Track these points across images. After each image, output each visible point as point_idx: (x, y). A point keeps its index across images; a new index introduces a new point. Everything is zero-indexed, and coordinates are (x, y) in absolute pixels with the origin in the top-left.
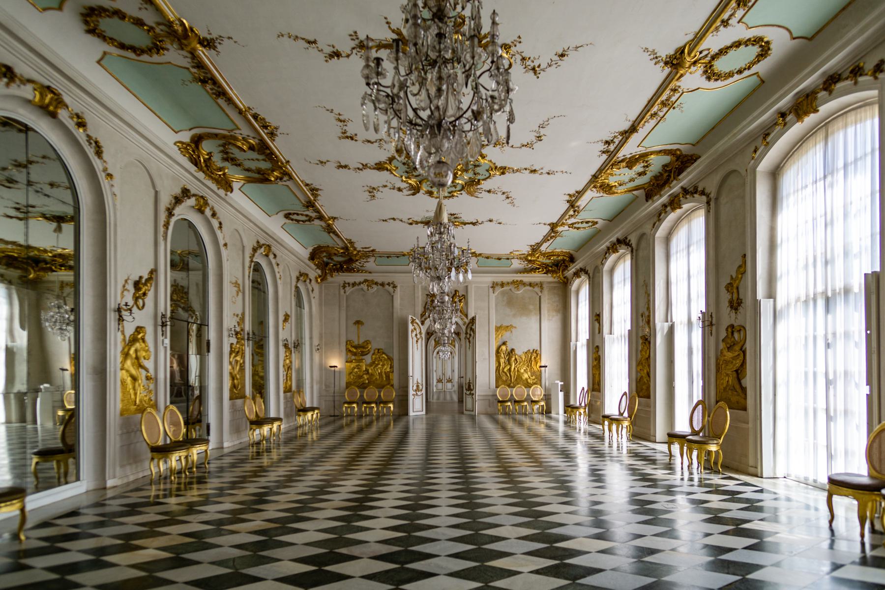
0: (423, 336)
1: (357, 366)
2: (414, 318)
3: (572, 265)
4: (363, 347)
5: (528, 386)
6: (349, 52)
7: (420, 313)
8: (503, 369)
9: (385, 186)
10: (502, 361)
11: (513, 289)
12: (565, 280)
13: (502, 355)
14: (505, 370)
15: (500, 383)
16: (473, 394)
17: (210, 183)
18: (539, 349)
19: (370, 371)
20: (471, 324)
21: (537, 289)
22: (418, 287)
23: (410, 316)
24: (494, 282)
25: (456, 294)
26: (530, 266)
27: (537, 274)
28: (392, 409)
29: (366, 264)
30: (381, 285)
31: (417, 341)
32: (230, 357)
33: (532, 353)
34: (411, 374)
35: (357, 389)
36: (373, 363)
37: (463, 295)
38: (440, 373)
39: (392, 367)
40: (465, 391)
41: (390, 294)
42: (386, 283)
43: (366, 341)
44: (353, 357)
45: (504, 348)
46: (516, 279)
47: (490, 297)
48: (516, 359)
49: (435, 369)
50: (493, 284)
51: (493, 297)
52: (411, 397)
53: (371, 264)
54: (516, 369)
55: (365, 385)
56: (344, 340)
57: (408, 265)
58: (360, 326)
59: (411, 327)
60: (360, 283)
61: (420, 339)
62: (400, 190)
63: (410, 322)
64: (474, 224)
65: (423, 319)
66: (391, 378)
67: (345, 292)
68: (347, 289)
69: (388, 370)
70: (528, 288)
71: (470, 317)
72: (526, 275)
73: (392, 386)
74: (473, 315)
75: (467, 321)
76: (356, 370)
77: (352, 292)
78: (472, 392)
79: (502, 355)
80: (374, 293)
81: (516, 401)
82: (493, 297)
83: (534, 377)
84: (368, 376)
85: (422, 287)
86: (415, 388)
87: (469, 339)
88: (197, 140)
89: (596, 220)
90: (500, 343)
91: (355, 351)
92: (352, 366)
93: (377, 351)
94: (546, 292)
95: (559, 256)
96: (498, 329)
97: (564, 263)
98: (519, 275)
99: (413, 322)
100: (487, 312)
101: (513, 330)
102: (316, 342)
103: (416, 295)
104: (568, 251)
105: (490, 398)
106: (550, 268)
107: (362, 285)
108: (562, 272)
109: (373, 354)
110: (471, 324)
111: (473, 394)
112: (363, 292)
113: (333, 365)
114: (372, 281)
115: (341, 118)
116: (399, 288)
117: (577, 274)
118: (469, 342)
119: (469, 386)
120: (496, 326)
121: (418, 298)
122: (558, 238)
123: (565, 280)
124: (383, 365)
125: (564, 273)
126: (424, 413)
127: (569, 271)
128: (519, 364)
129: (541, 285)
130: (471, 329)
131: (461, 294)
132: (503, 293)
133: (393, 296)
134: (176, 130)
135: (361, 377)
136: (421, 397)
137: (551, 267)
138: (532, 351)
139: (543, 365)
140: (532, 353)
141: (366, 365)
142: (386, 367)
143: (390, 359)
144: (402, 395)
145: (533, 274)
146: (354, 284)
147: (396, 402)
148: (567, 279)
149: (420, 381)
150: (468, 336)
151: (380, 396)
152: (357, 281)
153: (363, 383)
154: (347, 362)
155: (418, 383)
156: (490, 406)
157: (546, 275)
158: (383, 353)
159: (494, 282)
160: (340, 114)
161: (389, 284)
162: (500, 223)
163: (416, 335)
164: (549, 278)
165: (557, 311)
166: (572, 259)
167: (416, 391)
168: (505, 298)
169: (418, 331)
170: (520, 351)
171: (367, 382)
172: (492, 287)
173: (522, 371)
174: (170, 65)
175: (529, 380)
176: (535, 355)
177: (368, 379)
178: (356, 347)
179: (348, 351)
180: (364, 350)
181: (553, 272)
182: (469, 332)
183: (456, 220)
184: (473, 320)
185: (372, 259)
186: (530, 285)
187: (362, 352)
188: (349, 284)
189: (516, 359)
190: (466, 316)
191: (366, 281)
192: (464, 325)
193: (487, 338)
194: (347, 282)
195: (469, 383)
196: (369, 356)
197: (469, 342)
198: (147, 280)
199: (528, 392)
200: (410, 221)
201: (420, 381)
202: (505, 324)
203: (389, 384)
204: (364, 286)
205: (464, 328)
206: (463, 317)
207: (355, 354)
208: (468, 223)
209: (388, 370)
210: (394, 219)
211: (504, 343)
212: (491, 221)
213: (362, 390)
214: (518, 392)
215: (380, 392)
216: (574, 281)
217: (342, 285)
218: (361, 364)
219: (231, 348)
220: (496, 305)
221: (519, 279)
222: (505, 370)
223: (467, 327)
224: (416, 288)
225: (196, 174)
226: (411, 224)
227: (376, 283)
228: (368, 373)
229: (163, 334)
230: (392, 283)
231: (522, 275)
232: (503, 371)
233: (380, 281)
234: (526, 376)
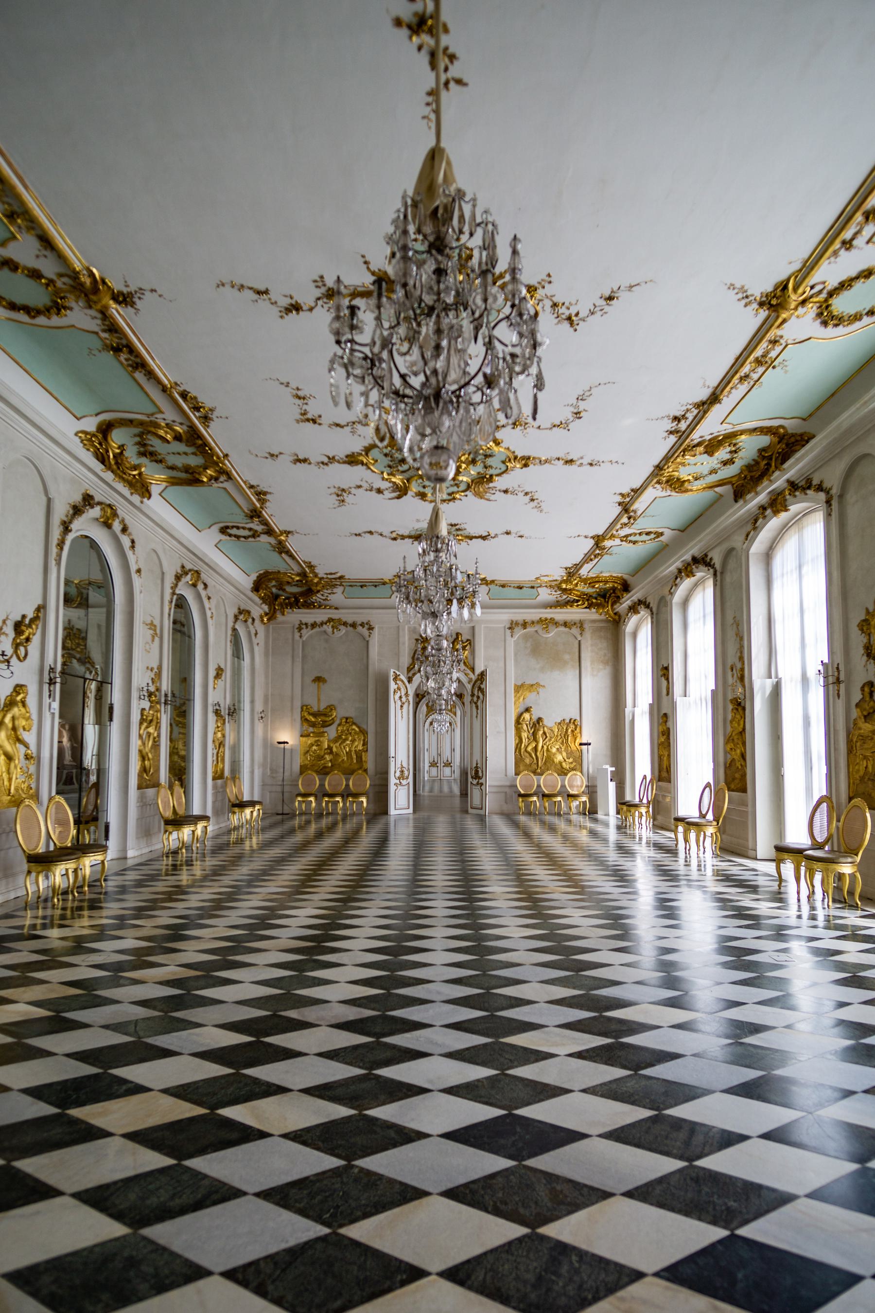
0: (411, 698)
1: (316, 741)
2: (398, 673)
3: (626, 596)
4: (325, 715)
5: (563, 772)
6: (313, 304)
7: (406, 665)
8: (526, 747)
9: (359, 487)
10: (524, 735)
11: (540, 631)
12: (617, 617)
13: (525, 727)
14: (529, 749)
15: (522, 768)
16: (482, 784)
17: (120, 487)
18: (578, 719)
19: (334, 749)
20: (479, 682)
21: (575, 631)
22: (404, 630)
23: (392, 671)
24: (512, 621)
25: (457, 638)
26: (565, 597)
27: (575, 609)
28: (365, 804)
29: (330, 597)
31: (402, 706)
32: (140, 728)
33: (568, 725)
34: (392, 754)
35: (315, 775)
36: (339, 737)
37: (468, 640)
38: (434, 753)
39: (365, 744)
40: (470, 780)
41: (364, 639)
42: (359, 623)
43: (329, 706)
44: (311, 729)
45: (527, 716)
46: (544, 616)
47: (507, 642)
48: (544, 733)
49: (426, 747)
50: (511, 624)
51: (511, 642)
52: (392, 788)
53: (337, 597)
54: (545, 747)
55: (327, 770)
56: (298, 704)
58: (321, 684)
59: (393, 686)
60: (322, 624)
61: (406, 704)
62: (379, 491)
63: (392, 678)
64: (484, 538)
65: (410, 675)
66: (364, 759)
67: (301, 637)
68: (304, 631)
69: (360, 747)
70: (562, 629)
71: (478, 671)
72: (558, 610)
73: (366, 771)
74: (482, 669)
75: (474, 678)
76: (314, 748)
77: (311, 636)
78: (481, 781)
79: (525, 727)
80: (341, 637)
81: (544, 795)
82: (511, 642)
83: (571, 760)
84: (331, 757)
85: (409, 628)
86: (398, 774)
87: (476, 703)
88: (105, 429)
89: (660, 530)
90: (522, 709)
91: (313, 720)
92: (309, 742)
93: (344, 720)
94: (588, 634)
95: (606, 582)
96: (518, 688)
97: (614, 592)
98: (549, 610)
99: (396, 678)
100: (502, 664)
101: (541, 690)
102: (259, 707)
103: (401, 640)
104: (620, 575)
105: (507, 790)
106: (594, 601)
107: (325, 626)
108: (612, 605)
109: (339, 725)
110: (479, 682)
111: (482, 784)
112: (326, 636)
113: (282, 740)
114: (339, 620)
115: (300, 393)
116: (376, 630)
117: (633, 609)
118: (477, 707)
119: (477, 772)
120: (515, 685)
121: (404, 644)
122: (605, 557)
123: (617, 617)
124: (353, 741)
125: (615, 607)
126: (411, 810)
127: (621, 604)
128: (550, 740)
129: (581, 625)
130: (480, 689)
131: (464, 638)
132: (526, 637)
134: (79, 416)
135: (321, 758)
136: (406, 787)
137: (596, 598)
138: (568, 721)
139: (584, 741)
140: (568, 725)
141: (329, 741)
142: (356, 743)
143: (363, 732)
144: (379, 785)
145: (569, 609)
146: (314, 625)
147: (371, 795)
148: (620, 616)
149: (405, 765)
150: (475, 699)
151: (347, 785)
152: (319, 620)
153: (325, 767)
154: (302, 736)
155: (402, 767)
156: (506, 802)
157: (587, 610)
158: (354, 724)
159: (512, 621)
160: (298, 389)
161: (362, 625)
162: (521, 536)
164: (592, 615)
165: (606, 663)
166: (626, 587)
167: (399, 778)
168: (529, 644)
169: (403, 692)
170: (550, 722)
171: (330, 765)
172: (510, 628)
173: (554, 750)
174: (72, 329)
175: (564, 764)
176: (572, 726)
177: (331, 761)
178: (314, 715)
179: (304, 720)
180: (327, 719)
181: (598, 606)
182: (476, 693)
183: (459, 533)
184: (482, 676)
185: (339, 590)
186: (565, 624)
187: (324, 722)
188: (306, 624)
189: (544, 733)
190: (473, 670)
191: (330, 620)
192: (470, 681)
193: (502, 702)
194: (304, 622)
195: (477, 767)
196: (334, 727)
197: (477, 707)
198: (32, 621)
199: (563, 781)
200: (394, 535)
201: (405, 765)
202: (528, 682)
203: (361, 768)
204: (328, 628)
205: (469, 687)
206: (468, 671)
207: (313, 725)
208: (476, 537)
209: (360, 747)
210: (371, 533)
211: (527, 710)
212: (508, 533)
213: (321, 776)
214: (548, 781)
215: (347, 780)
216: (629, 619)
218: (321, 739)
219: (142, 715)
220: (516, 655)
221: (549, 616)
222: (529, 749)
223: (474, 685)
225: (102, 474)
226: (395, 539)
227: (345, 624)
228: (331, 752)
229: (50, 696)
231: (553, 610)
232: (526, 751)
233: (350, 621)
234: (559, 758)
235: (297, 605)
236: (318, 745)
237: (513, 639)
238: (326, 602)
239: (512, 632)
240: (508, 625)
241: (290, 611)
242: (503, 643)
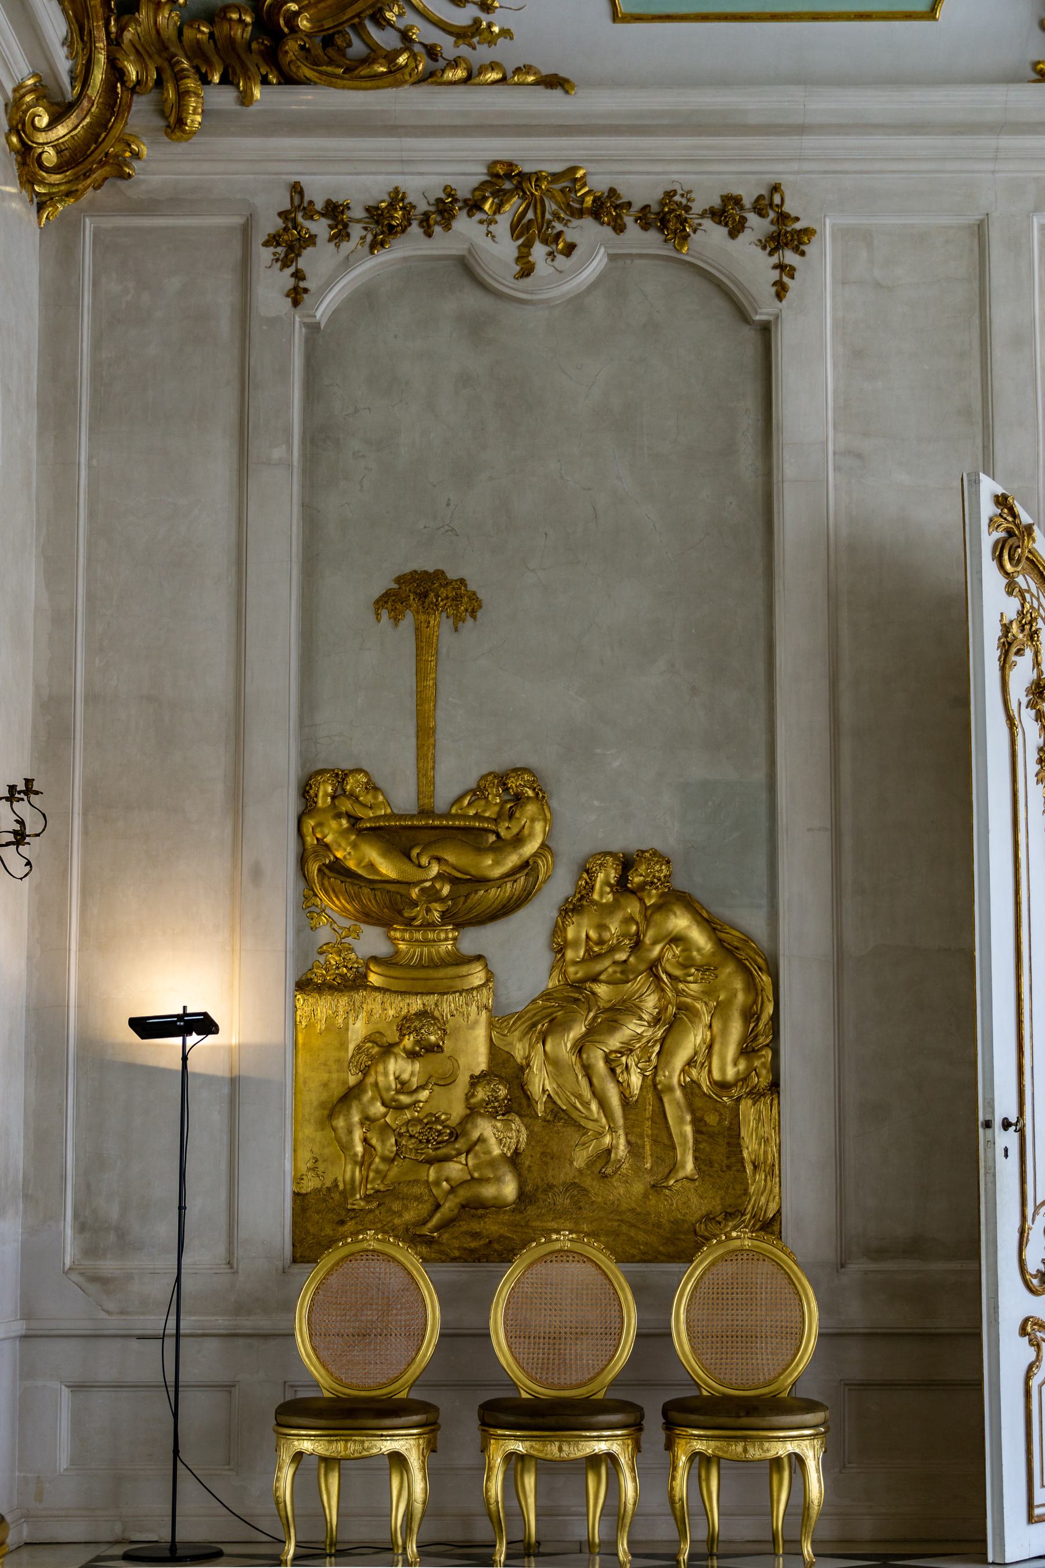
1: (405, 1024)
30: (646, 219)
35: (410, 1259)
42: (706, 198)
43: (501, 779)
55: (491, 1227)
58: (441, 625)
63: (988, 540)
66: (750, 1147)
67: (296, 295)
76: (397, 1067)
80: (577, 303)
84: (518, 1133)
91: (387, 869)
92: (358, 1029)
107: (464, 225)
112: (473, 300)
113: (168, 1006)
133: (766, 330)
141: (498, 1020)
153: (475, 1207)
154: (303, 985)
171: (509, 1189)
177: (514, 1160)
180: (492, 866)
188: (334, 211)
194: (317, 193)
203: (732, 1213)
213: (452, 1272)
217: (271, 224)
218: (448, 1005)
230: (760, 207)
235: (272, 57)
236: (425, 1051)
238: (483, 53)
241: (224, 98)
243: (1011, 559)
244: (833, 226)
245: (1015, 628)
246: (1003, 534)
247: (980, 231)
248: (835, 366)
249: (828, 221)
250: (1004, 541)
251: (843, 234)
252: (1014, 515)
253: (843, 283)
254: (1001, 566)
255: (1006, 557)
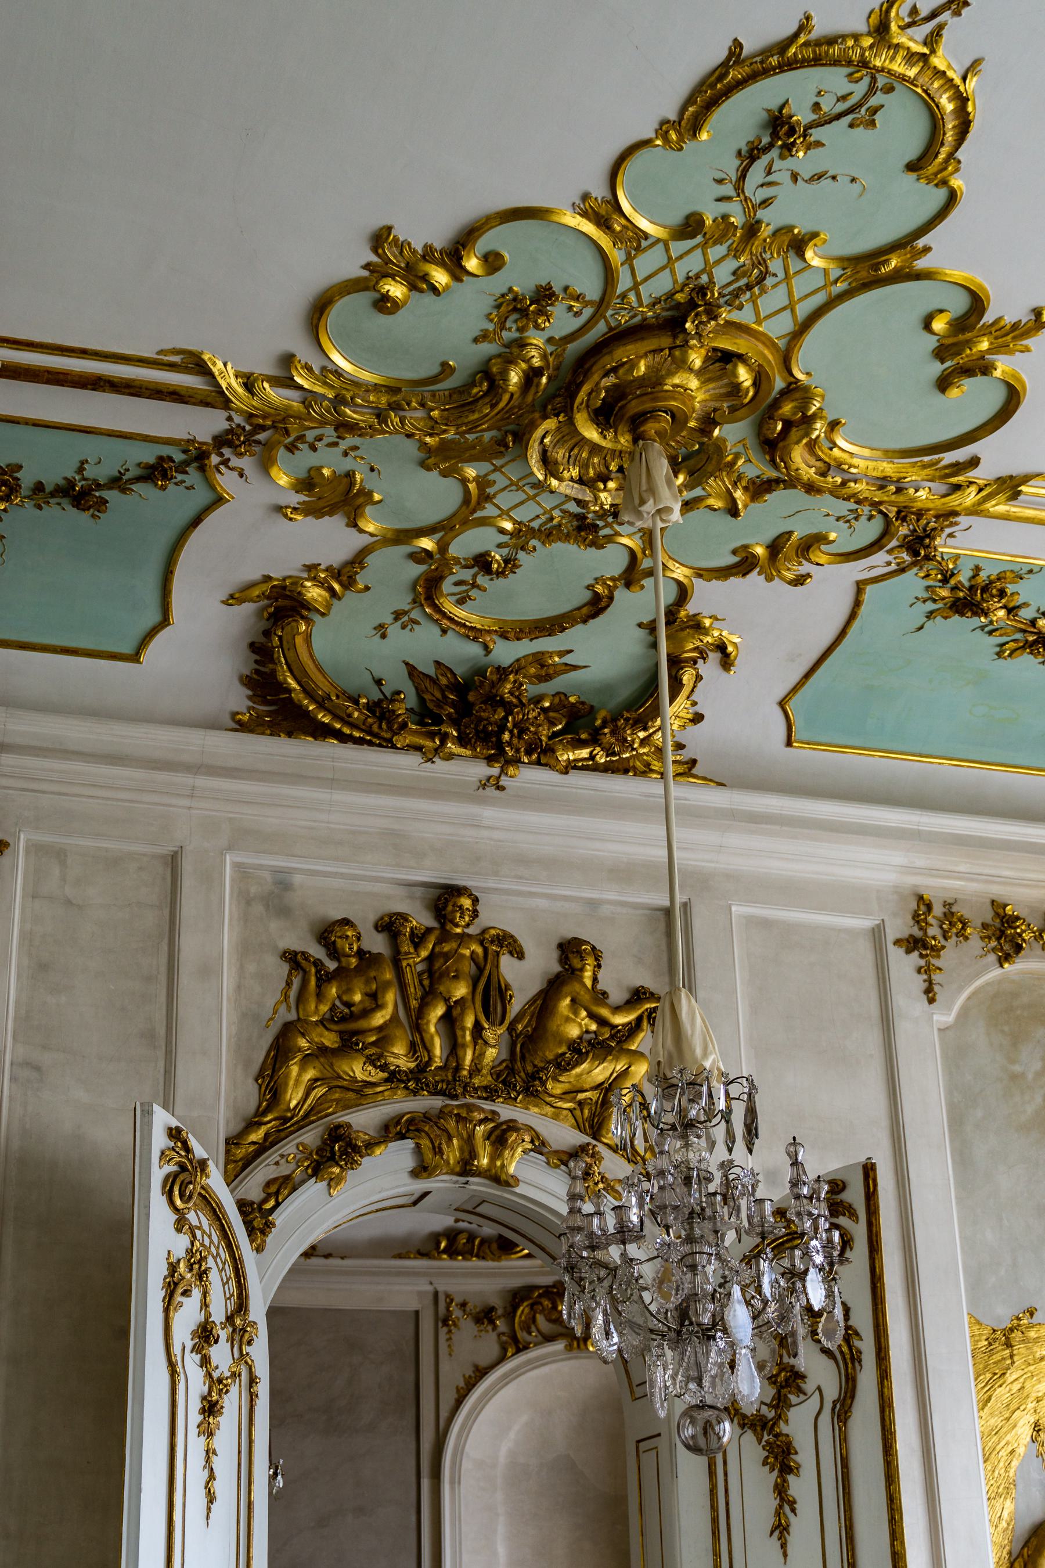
22: (210, 878)
24: (924, 904)
47: (904, 1030)
57: (135, 657)
65: (253, 1186)
103: (190, 944)
121: (208, 970)
163: (205, 1335)
220: (957, 1120)
224: (188, 884)
237: (944, 1016)
239: (926, 970)
240: (900, 926)
242: (873, 1039)
243: (181, 1196)
244: (27, 841)
245: (182, 1267)
246: (175, 1168)
247: (173, 862)
248: (19, 976)
249: (22, 836)
250: (176, 1175)
251: (36, 849)
252: (187, 1149)
253: (33, 897)
254: (171, 1202)
255: (176, 1193)
